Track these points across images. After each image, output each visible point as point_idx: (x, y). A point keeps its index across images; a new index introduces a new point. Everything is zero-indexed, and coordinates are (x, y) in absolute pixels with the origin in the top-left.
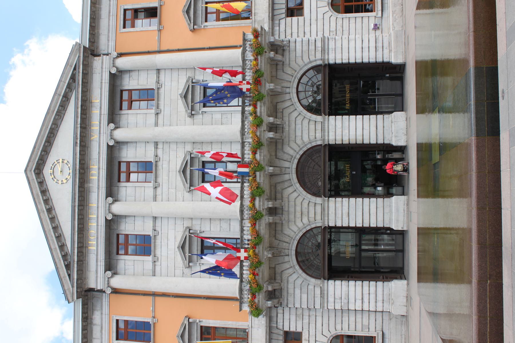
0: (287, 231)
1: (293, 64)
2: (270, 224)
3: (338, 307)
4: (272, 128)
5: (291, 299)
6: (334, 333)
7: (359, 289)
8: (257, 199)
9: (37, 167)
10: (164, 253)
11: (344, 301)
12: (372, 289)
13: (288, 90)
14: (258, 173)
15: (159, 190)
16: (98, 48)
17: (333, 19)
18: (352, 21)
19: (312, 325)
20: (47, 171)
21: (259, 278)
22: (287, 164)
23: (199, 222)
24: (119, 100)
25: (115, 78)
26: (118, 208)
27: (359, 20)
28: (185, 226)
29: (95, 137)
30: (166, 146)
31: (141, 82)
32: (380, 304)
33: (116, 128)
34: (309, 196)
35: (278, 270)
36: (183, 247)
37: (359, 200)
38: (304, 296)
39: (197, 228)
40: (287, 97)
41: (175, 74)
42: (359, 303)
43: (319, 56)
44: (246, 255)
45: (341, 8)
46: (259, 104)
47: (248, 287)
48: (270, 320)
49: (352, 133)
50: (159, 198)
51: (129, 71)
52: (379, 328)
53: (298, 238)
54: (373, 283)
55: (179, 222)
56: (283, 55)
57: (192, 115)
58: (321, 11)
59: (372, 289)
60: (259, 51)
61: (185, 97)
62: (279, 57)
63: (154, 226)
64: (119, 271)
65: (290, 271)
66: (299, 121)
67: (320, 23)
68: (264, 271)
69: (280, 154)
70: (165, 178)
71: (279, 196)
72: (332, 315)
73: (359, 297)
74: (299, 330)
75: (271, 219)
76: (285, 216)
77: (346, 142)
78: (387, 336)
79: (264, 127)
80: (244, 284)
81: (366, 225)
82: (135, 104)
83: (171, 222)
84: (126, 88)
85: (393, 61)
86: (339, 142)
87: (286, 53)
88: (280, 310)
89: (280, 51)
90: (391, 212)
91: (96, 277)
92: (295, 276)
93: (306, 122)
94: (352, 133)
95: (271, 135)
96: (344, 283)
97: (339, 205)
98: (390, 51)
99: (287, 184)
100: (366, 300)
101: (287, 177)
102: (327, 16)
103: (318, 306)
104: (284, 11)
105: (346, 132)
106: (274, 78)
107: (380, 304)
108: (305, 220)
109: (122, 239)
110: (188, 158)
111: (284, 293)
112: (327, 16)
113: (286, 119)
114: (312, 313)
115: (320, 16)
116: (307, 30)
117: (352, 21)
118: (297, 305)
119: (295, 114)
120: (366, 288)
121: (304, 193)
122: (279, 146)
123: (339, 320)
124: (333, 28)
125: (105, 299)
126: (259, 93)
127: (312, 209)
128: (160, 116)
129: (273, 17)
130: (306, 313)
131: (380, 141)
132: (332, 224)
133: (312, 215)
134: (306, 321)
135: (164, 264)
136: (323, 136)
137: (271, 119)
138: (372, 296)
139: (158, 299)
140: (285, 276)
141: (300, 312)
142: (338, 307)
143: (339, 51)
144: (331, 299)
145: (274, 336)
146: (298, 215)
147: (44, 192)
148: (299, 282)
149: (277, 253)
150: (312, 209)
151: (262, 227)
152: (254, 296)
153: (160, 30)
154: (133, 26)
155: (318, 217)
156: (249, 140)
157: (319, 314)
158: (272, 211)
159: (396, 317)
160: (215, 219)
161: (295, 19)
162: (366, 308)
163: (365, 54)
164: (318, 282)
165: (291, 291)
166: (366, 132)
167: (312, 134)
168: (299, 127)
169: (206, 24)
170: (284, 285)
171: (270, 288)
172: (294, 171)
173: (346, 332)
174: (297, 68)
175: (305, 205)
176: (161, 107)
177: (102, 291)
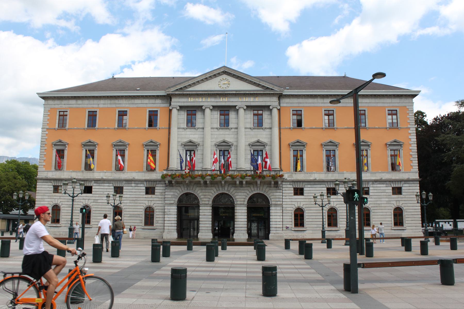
0: (197, 189)
1: (270, 191)
2: (200, 182)
3: (166, 210)
4: (241, 183)
5: (169, 190)
6: (155, 208)
7: (174, 219)
8: (210, 177)
9: (226, 72)
10: (188, 133)
11: (168, 213)
12: (173, 225)
13: (259, 189)
14: (221, 177)
15: (216, 130)
16: (283, 98)
17: (292, 209)
18: (290, 217)
19: (158, 199)
20: (225, 76)
21: (177, 178)
22: (226, 189)
23: (202, 149)
24: (257, 110)
25: (267, 108)
26: (208, 111)
27: (291, 220)
28: (200, 143)
29: (240, 100)
30: (236, 133)
31: (266, 120)
32: (167, 228)
33: (245, 110)
34: (212, 198)
35: (181, 185)
36: (190, 142)
37: (211, 220)
38: (170, 196)
39: (199, 148)
40: (256, 189)
41: (269, 136)
42: (168, 219)
43: (273, 203)
44: (187, 172)
45: (297, 212)
46: (251, 178)
47: (173, 173)
48: (160, 181)
49: (240, 217)
50: (213, 130)
51: (271, 114)
52: (157, 227)
53: (195, 194)
54: (176, 225)
55: (202, 140)
56: (274, 187)
57: (249, 145)
58: (296, 204)
59: (173, 225)
60: (274, 177)
61: (258, 142)
62: (272, 186)
63: (200, 128)
64: (180, 111)
65: (181, 190)
66: (245, 194)
67: (290, 203)
68: (180, 179)
69: (230, 186)
70: (222, 133)
71: (213, 185)
72: (162, 208)
73: (170, 219)
74: (156, 194)
75: (202, 182)
76: (204, 188)
77: (236, 214)
78: (154, 231)
79: (241, 180)
80: (175, 172)
81: (200, 222)
82: (256, 117)
83: (202, 136)
84: (264, 113)
85: (270, 235)
86: (235, 211)
87: (275, 189)
88: (164, 185)
89: (276, 186)
90: (206, 233)
91: (177, 102)
92: (179, 192)
93: (244, 197)
94: (240, 217)
95: (238, 183)
96: (176, 213)
97: (209, 211)
98: (275, 233)
99: (217, 189)
100: (169, 222)
101: (221, 189)
102: (293, 206)
103: (166, 202)
104: (296, 187)
105: (240, 214)
106: (263, 183)
107: (167, 228)
108: (202, 197)
109: (193, 112)
110: (230, 144)
111: (171, 188)
112: (293, 206)
113: (246, 188)
114: (163, 199)
115: (293, 203)
116: (287, 197)
117: (290, 217)
118: (166, 193)
119: (248, 192)
120: (174, 222)
121: (214, 196)
122: (234, 185)
123: (160, 211)
124: (287, 209)
125: (168, 105)
126: (255, 178)
127: (207, 199)
128: (250, 130)
129: (294, 182)
130: (163, 197)
131: (236, 229)
132: (201, 208)
133: (204, 199)
134: (160, 196)
135: (183, 133)
136: (238, 204)
137: (244, 183)
138: (170, 225)
139: (168, 130)
140: (179, 188)
141: (163, 194)
142: (166, 210)
143: (275, 211)
144: (169, 208)
145: (153, 183)
146: (204, 194)
147: (215, 76)
148: (176, 194)
149: (188, 185)
150: (207, 199)
151: (198, 179)
152: (170, 176)
153: (290, 128)
154: (293, 115)
155: (203, 202)
156: (236, 173)
157: (163, 202)
158: (205, 183)
159: (162, 235)
160: (203, 156)
161: (293, 192)
162: (165, 222)
163: (274, 223)
164: (176, 202)
165: (172, 191)
166: (239, 223)
167: (239, 200)
168: (242, 194)
169: (292, 151)
170: (175, 188)
171: (173, 182)
172: (223, 192)
173: (155, 214)
174: (269, 193)
175: (209, 197)
176: (254, 130)
177: (170, 105)
